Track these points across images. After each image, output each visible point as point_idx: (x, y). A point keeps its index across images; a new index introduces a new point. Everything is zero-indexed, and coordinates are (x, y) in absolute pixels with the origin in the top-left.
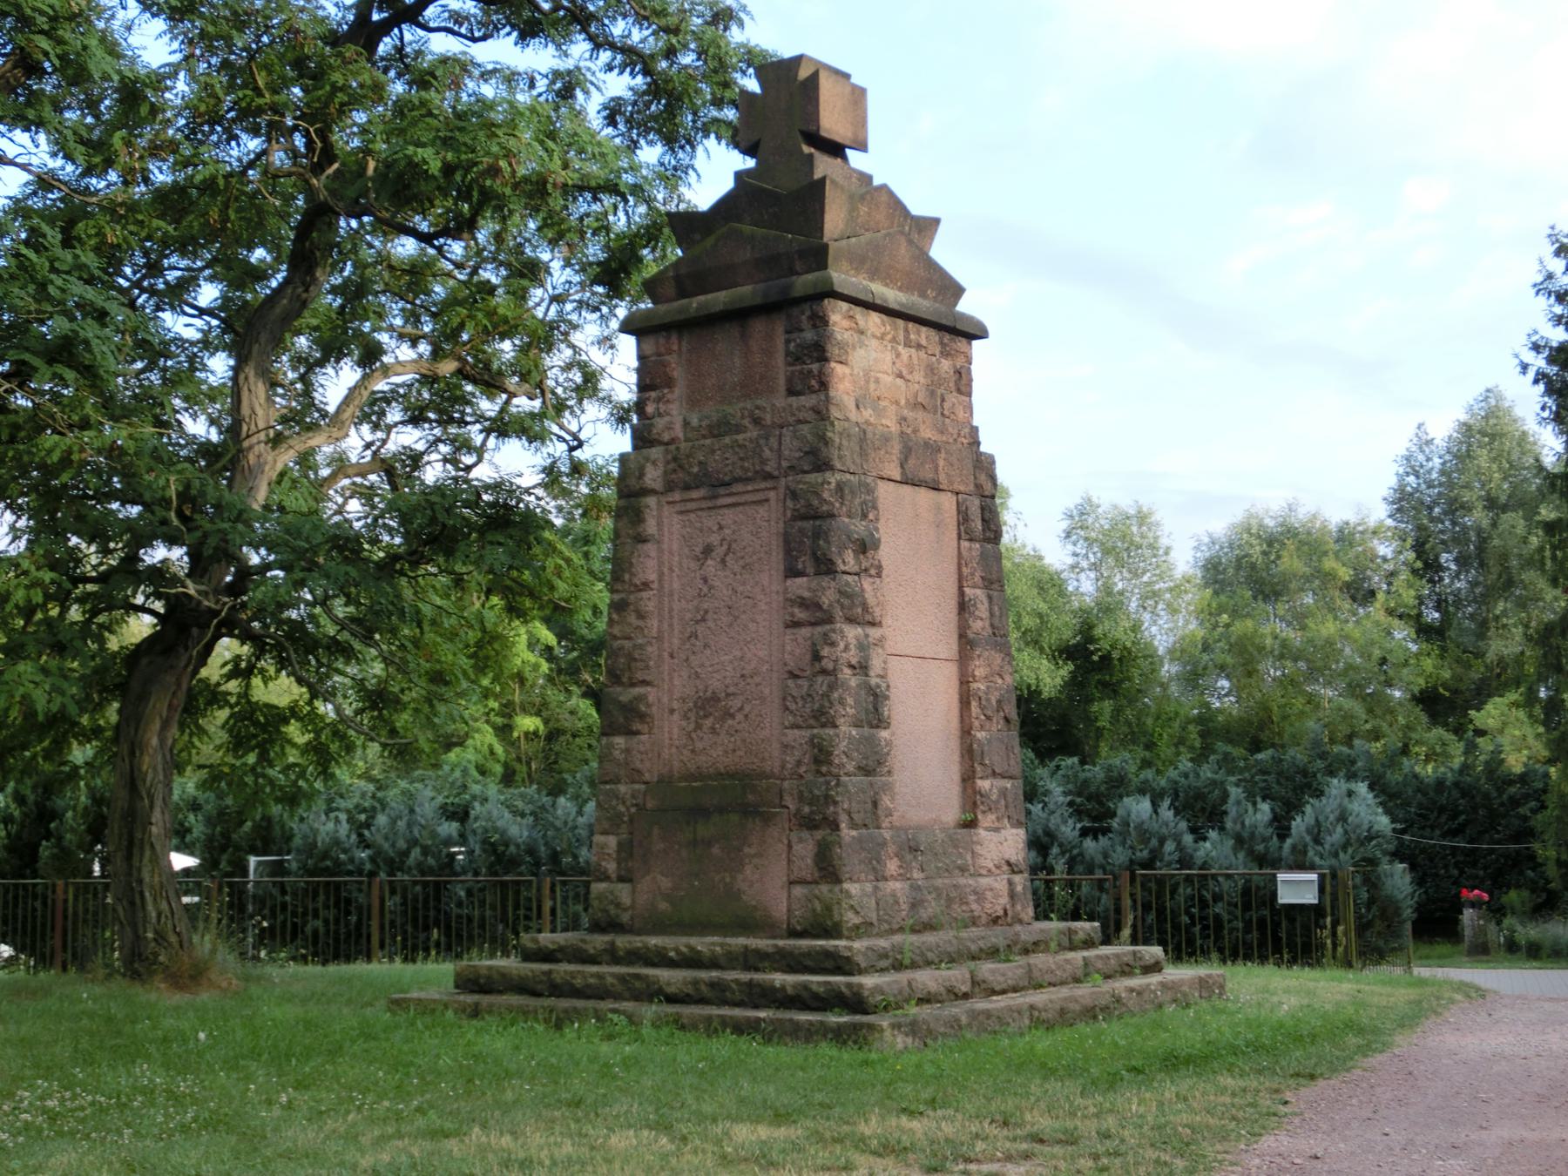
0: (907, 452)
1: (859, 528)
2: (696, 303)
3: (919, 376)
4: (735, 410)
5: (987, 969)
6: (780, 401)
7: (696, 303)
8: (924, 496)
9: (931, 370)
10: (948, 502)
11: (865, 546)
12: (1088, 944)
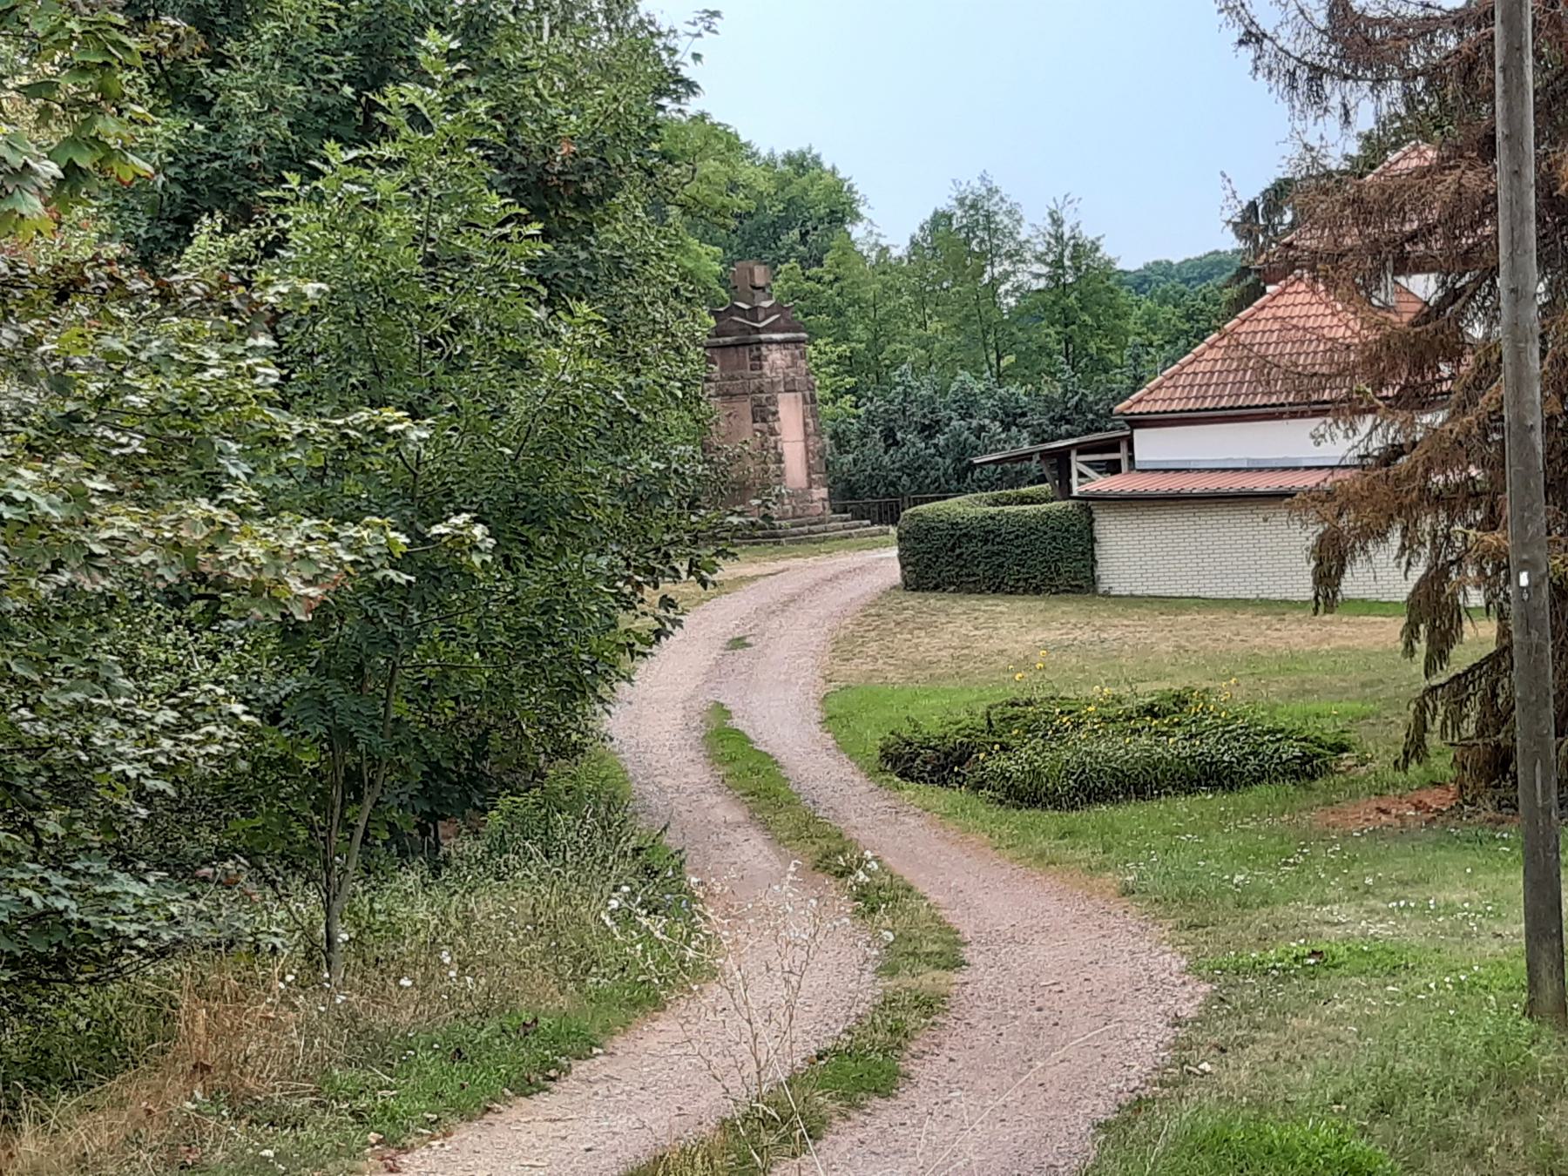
0: (786, 383)
1: (772, 409)
2: (721, 340)
3: (789, 358)
4: (736, 373)
5: (812, 528)
6: (749, 371)
7: (721, 340)
8: (792, 394)
9: (792, 355)
10: (799, 395)
11: (775, 413)
12: (846, 520)
